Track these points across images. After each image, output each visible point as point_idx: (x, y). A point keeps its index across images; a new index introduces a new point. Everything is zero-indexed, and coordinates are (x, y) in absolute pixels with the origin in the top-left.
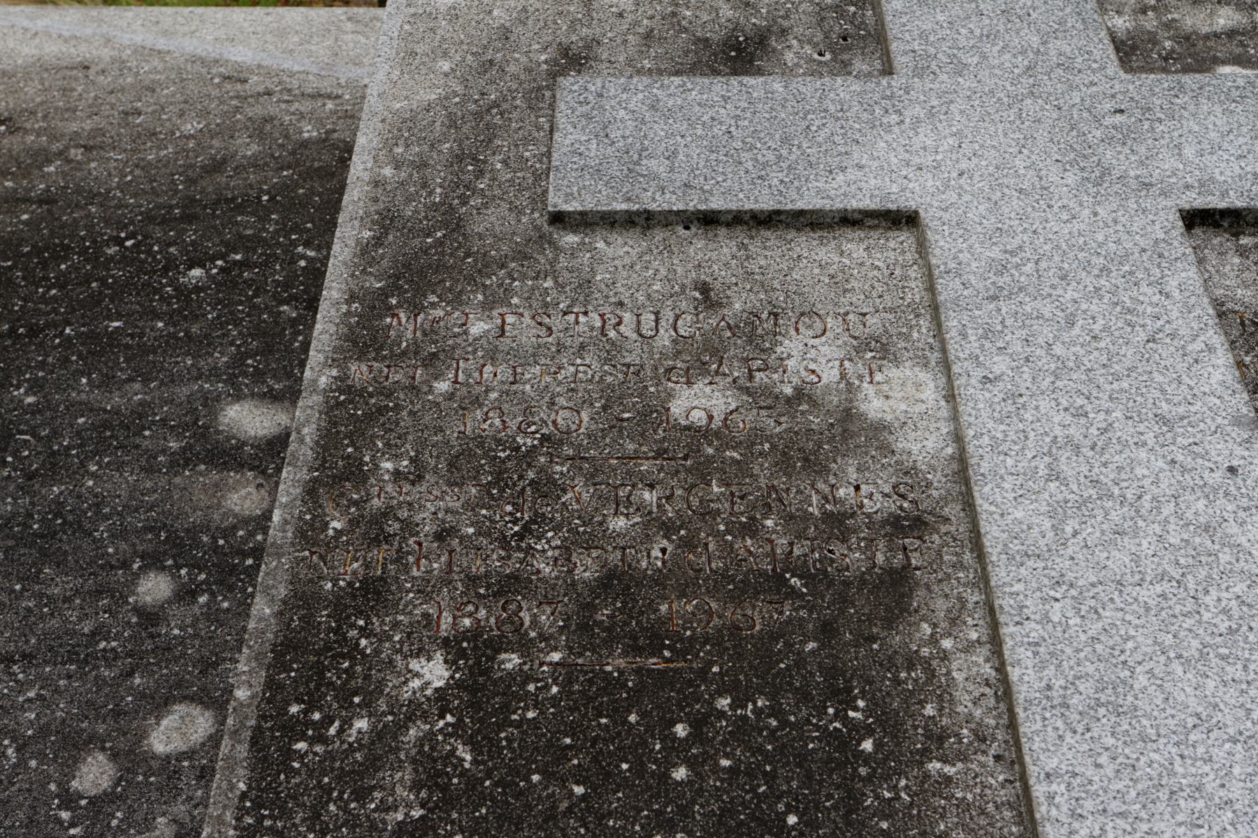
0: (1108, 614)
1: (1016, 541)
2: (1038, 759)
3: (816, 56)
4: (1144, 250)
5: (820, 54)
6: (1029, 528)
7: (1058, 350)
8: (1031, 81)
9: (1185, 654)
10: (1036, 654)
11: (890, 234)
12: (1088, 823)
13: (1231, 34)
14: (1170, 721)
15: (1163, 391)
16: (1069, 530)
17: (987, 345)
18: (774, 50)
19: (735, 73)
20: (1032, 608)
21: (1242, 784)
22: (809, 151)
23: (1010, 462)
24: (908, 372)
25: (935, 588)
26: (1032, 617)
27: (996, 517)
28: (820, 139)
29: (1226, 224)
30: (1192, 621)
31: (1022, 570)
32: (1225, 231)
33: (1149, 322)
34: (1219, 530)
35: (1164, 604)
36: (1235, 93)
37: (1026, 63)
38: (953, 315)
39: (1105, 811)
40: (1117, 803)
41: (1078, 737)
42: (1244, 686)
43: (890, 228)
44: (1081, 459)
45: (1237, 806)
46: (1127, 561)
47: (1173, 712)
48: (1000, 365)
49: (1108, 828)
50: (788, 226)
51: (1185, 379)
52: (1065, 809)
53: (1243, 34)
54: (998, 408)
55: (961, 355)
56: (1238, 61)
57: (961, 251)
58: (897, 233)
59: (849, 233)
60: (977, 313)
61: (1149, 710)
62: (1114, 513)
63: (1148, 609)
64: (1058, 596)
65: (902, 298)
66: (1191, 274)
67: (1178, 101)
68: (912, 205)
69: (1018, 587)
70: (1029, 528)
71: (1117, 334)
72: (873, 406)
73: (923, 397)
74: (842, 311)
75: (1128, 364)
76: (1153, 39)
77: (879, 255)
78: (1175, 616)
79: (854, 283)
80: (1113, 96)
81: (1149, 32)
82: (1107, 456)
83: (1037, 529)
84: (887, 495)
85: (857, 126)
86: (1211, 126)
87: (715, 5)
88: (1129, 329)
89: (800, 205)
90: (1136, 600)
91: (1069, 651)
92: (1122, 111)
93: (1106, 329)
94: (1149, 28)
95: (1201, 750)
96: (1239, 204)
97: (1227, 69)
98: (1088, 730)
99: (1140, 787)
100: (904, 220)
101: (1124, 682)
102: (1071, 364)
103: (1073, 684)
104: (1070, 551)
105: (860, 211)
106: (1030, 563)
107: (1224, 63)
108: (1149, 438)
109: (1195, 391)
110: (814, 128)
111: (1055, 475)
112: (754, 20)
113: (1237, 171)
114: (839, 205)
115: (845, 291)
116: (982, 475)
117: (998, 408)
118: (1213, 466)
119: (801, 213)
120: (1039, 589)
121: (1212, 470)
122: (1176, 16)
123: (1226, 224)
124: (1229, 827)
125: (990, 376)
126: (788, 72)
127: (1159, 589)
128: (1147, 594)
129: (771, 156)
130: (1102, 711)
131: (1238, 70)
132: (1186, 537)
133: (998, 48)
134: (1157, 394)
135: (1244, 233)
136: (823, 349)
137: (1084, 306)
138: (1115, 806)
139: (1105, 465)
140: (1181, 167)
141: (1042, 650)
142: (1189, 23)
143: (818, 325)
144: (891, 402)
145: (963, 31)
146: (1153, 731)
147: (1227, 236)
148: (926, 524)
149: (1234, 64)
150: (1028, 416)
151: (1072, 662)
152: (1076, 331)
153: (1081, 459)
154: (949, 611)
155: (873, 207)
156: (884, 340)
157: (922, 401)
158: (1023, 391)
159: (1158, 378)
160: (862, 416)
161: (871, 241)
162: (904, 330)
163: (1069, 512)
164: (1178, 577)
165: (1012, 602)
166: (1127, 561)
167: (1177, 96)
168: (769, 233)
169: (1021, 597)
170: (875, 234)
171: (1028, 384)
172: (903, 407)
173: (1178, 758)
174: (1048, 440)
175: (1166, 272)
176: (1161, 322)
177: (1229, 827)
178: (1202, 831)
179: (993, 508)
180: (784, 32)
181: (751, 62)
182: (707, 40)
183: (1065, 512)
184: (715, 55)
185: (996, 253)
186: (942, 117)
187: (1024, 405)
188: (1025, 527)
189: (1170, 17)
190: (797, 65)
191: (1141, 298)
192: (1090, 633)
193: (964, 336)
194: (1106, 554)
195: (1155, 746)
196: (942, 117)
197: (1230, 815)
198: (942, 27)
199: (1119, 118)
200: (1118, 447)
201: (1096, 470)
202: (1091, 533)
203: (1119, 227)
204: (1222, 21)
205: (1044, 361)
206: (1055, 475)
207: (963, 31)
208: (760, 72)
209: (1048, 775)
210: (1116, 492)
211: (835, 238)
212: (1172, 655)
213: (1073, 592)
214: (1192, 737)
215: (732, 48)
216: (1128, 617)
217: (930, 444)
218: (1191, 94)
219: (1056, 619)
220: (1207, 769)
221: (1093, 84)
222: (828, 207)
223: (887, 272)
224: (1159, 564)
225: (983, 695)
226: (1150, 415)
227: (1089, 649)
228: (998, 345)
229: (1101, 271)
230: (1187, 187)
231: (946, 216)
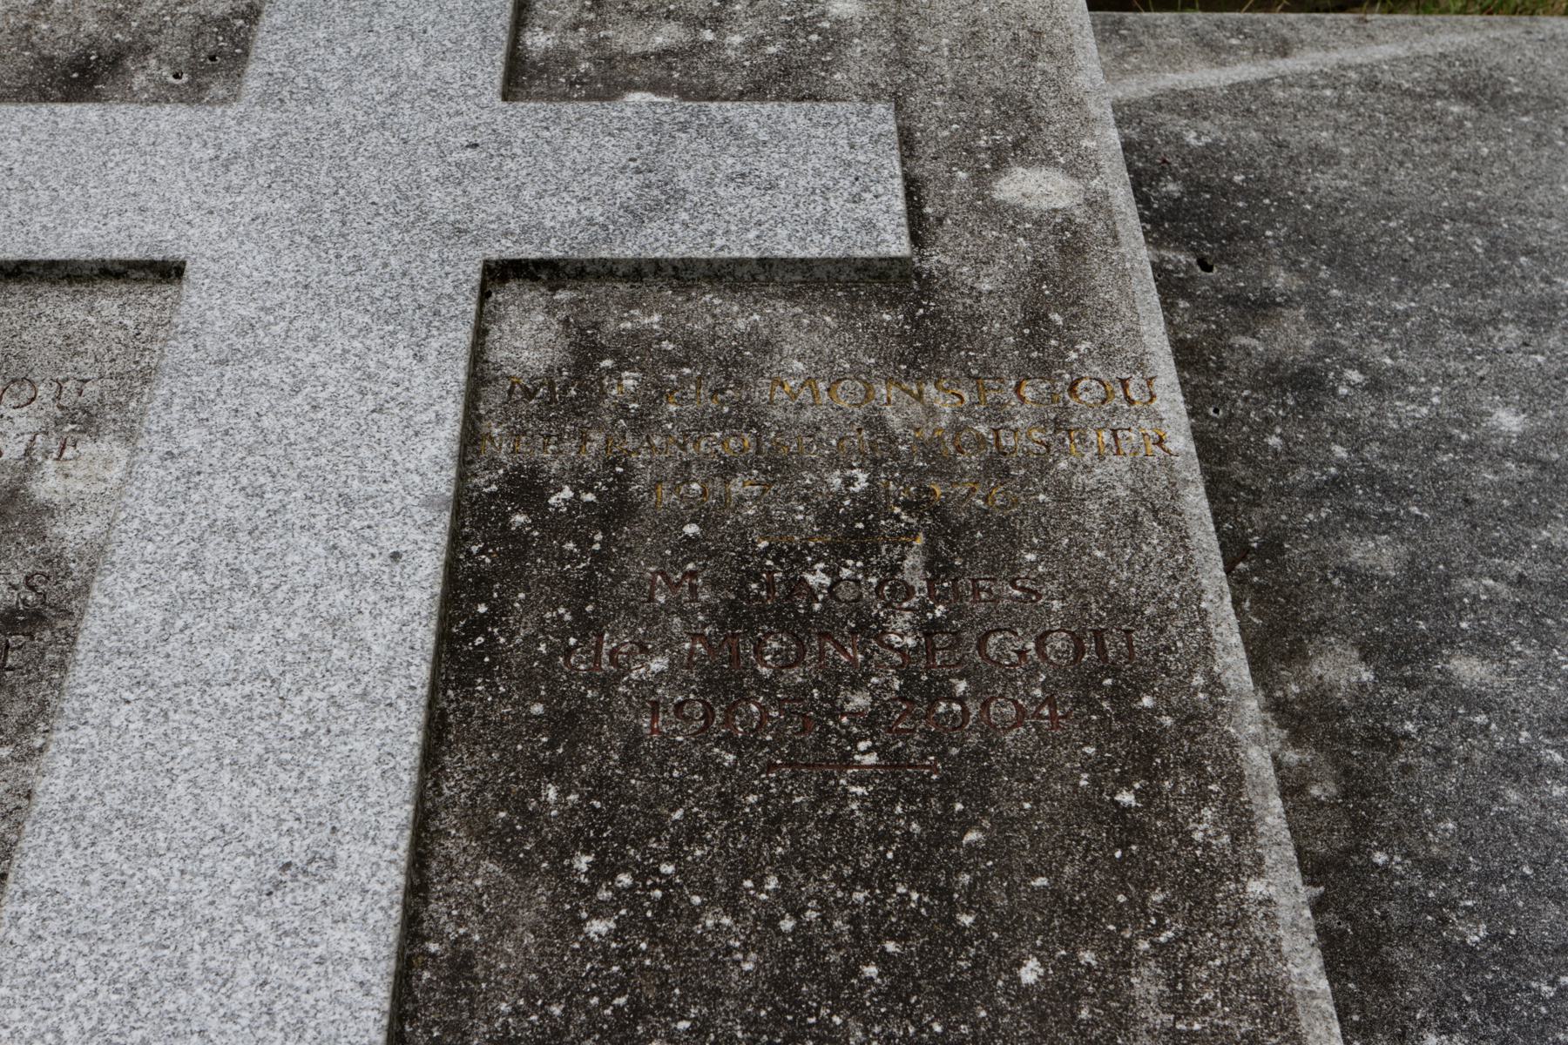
0: (177, 717)
1: (114, 637)
2: (23, 876)
3: (171, 79)
4: (420, 307)
5: (176, 76)
6: (136, 622)
7: (266, 422)
8: (389, 110)
9: (242, 760)
10: (75, 761)
11: (158, 288)
12: (44, 945)
13: (663, 54)
14: (190, 834)
15: (362, 468)
16: (180, 624)
17: (190, 415)
18: (126, 71)
19: (67, 99)
20: (96, 712)
21: (234, 901)
22: (92, 191)
23: (151, 547)
24: (104, 447)
25: (20, 691)
26: (91, 721)
27: (105, 610)
28: (112, 178)
29: (544, 277)
30: (267, 724)
31: (106, 670)
32: (544, 284)
33: (385, 389)
34: (348, 623)
35: (246, 706)
36: (616, 124)
37: (394, 88)
38: (166, 380)
39: (69, 932)
40: (88, 922)
41: (79, 851)
42: (289, 795)
43: (159, 282)
44: (233, 545)
45: (218, 925)
46: (227, 657)
47: (197, 823)
48: (192, 439)
49: (63, 950)
50: (42, 279)
51: (395, 455)
52: (25, 931)
53: (676, 55)
54: (167, 487)
55: (154, 428)
56: (656, 87)
57: (211, 308)
58: (166, 287)
59: (112, 287)
60: (195, 379)
61: (171, 822)
62: (239, 605)
63: (224, 711)
64: (131, 697)
65: (137, 363)
66: (459, 334)
67: (546, 134)
68: (182, 254)
69: (92, 688)
70: (136, 622)
71: (341, 403)
72: (47, 485)
73: (107, 475)
74: (60, 377)
75: (338, 436)
76: (570, 59)
77: (132, 313)
78: (251, 719)
79: (90, 346)
80: (474, 128)
81: (570, 52)
82: (263, 541)
83: (144, 623)
84: (15, 587)
85: (162, 162)
86: (568, 164)
87: (80, 12)
88: (358, 397)
89: (53, 255)
90: (216, 701)
91: (114, 758)
92: (476, 145)
93: (333, 398)
94: (572, 47)
95: (208, 864)
96: (555, 254)
97: (636, 97)
98: (93, 844)
99: (120, 905)
100: (169, 272)
101: (158, 792)
102: (273, 438)
103: (101, 794)
104: (168, 648)
105: (121, 262)
106: (119, 662)
107: (637, 88)
108: (320, 523)
109: (398, 468)
110: (110, 165)
111: (194, 564)
112: (118, 36)
113: (573, 214)
114: (97, 255)
115: (76, 353)
116: (113, 564)
117: (167, 487)
118: (376, 551)
119: (52, 264)
120: (114, 691)
121: (373, 556)
122: (610, 33)
123: (544, 277)
124: (197, 947)
125: (176, 452)
126: (130, 97)
127: (247, 689)
128: (230, 696)
129: (45, 197)
130: (119, 823)
131: (650, 97)
132: (306, 631)
133: (370, 70)
134: (354, 470)
135: (564, 287)
136: (17, 421)
137: (320, 371)
138: (84, 926)
139: (255, 552)
140: (511, 210)
141: (84, 757)
142: (621, 41)
143: (27, 392)
144: (69, 481)
145: (340, 50)
146: (165, 845)
147: (543, 290)
148: (44, 618)
149: (649, 90)
150: (196, 497)
151: (111, 770)
152: (299, 399)
153: (233, 545)
154: (24, 716)
155: (136, 256)
156: (93, 412)
157: (105, 480)
158: (205, 468)
159: (364, 452)
160: (30, 496)
161: (132, 297)
162: (122, 399)
163: (190, 604)
164: (275, 675)
165: (77, 705)
166: (227, 657)
167: (547, 129)
168: (17, 287)
169: (90, 699)
170: (138, 288)
171: (214, 461)
172: (80, 486)
173: (177, 874)
174: (205, 523)
175: (435, 332)
176: (399, 390)
177: (197, 947)
178: (166, 952)
179: (106, 601)
180: (147, 49)
181: (91, 86)
182: (52, 58)
183: (185, 603)
184: (53, 77)
185: (250, 311)
186: (265, 152)
187: (197, 484)
188: (131, 621)
189: (602, 34)
190: (145, 89)
191: (390, 362)
192: (146, 739)
193: (167, 405)
194: (208, 651)
195: (158, 861)
196: (265, 152)
197: (204, 934)
198: (318, 45)
199: (469, 153)
200: (280, 532)
201: (243, 558)
202: (202, 629)
203: (406, 281)
204: (659, 40)
205: (245, 434)
206: (194, 564)
207: (340, 50)
208: (97, 98)
209: (25, 894)
210: (254, 581)
211: (91, 292)
212: (227, 761)
213: (151, 693)
214: (205, 851)
215: (77, 69)
216: (199, 720)
217: (89, 529)
218: (564, 126)
219: (116, 723)
220: (204, 885)
221: (458, 113)
222: (83, 257)
223: (132, 332)
224: (262, 661)
225: (18, 808)
226: (335, 495)
227: (137, 756)
228: (202, 416)
229: (360, 330)
230: (506, 234)
231: (214, 267)
